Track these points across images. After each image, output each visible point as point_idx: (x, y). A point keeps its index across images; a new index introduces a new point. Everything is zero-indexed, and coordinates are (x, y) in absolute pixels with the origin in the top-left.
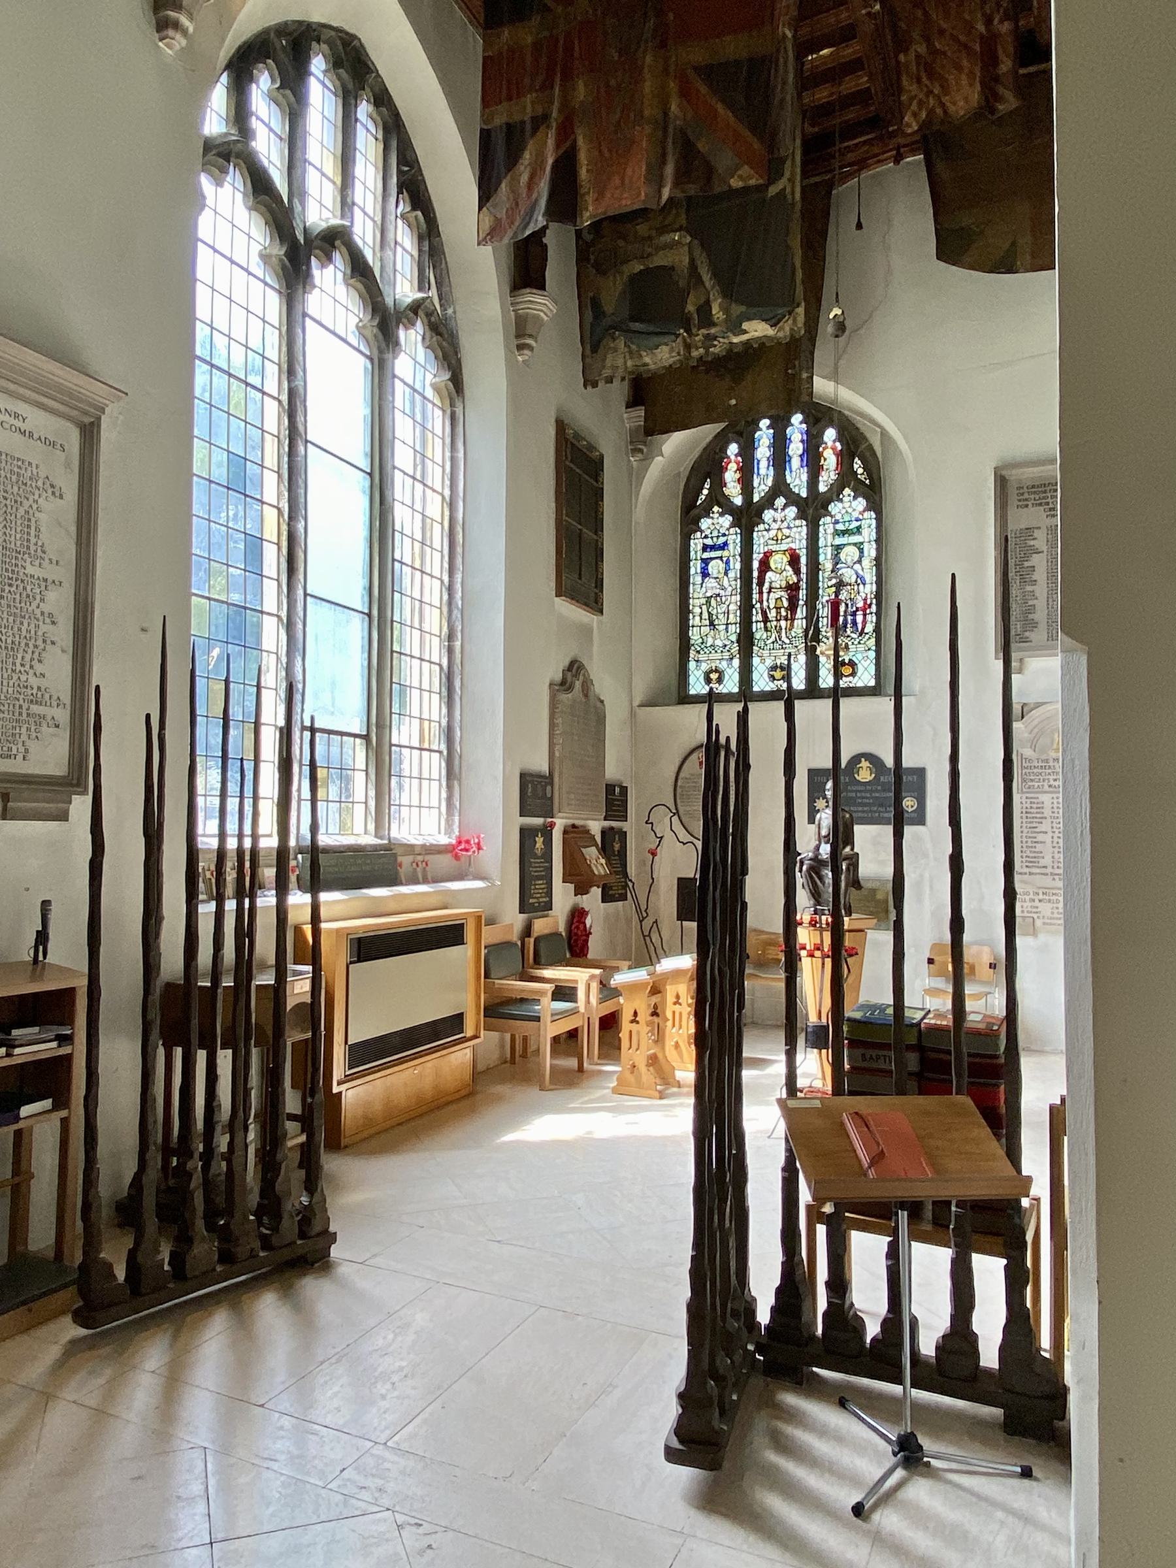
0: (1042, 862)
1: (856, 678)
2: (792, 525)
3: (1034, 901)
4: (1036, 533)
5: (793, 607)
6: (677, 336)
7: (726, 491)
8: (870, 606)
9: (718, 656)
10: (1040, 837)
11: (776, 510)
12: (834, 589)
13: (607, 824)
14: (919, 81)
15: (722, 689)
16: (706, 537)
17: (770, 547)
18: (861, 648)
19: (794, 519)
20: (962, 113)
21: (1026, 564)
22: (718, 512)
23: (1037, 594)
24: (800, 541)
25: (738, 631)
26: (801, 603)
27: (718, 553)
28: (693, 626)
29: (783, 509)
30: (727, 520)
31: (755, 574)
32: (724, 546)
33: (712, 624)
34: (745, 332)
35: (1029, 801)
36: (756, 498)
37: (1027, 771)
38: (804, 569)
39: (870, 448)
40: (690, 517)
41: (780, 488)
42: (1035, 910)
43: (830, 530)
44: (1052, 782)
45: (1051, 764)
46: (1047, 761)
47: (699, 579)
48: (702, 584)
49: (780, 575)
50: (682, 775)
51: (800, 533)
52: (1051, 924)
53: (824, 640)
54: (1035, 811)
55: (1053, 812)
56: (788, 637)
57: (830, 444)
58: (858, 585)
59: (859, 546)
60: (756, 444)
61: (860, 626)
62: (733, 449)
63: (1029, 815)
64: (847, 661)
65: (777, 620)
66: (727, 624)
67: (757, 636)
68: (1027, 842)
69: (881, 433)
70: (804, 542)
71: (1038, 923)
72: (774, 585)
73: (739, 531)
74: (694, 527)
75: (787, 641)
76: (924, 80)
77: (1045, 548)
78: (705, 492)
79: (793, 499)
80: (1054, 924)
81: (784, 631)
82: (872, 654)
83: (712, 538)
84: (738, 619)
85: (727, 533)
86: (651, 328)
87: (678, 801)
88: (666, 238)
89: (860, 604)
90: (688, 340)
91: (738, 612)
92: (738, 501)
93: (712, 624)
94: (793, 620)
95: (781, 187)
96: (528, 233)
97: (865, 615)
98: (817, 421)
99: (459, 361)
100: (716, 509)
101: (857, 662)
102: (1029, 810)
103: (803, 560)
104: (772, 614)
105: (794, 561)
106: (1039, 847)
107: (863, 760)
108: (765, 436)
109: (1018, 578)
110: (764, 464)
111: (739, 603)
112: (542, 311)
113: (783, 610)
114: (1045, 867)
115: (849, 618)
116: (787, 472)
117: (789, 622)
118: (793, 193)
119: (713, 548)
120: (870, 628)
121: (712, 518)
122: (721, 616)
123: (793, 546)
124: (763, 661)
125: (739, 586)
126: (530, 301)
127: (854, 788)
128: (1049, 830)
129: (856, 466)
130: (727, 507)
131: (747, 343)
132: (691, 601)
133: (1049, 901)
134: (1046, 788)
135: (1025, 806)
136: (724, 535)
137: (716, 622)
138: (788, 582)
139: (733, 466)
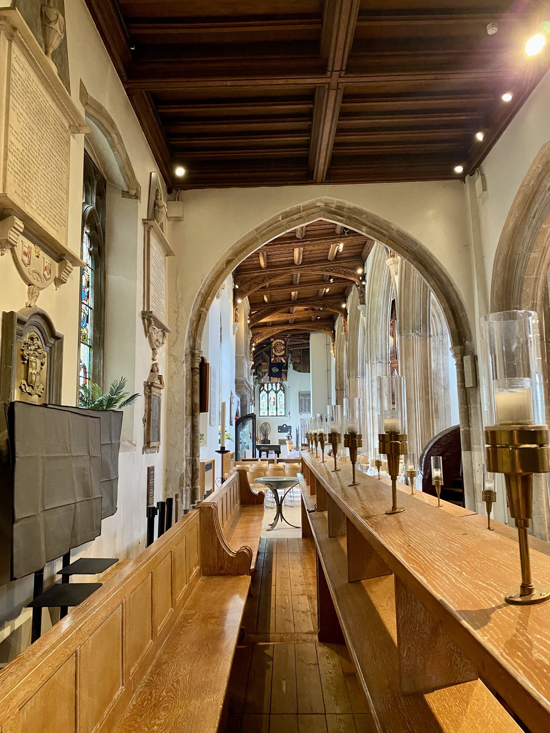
40: (260, 392)
41: (272, 389)
49: (272, 400)
79: (274, 391)
92: (267, 390)
130: (265, 391)
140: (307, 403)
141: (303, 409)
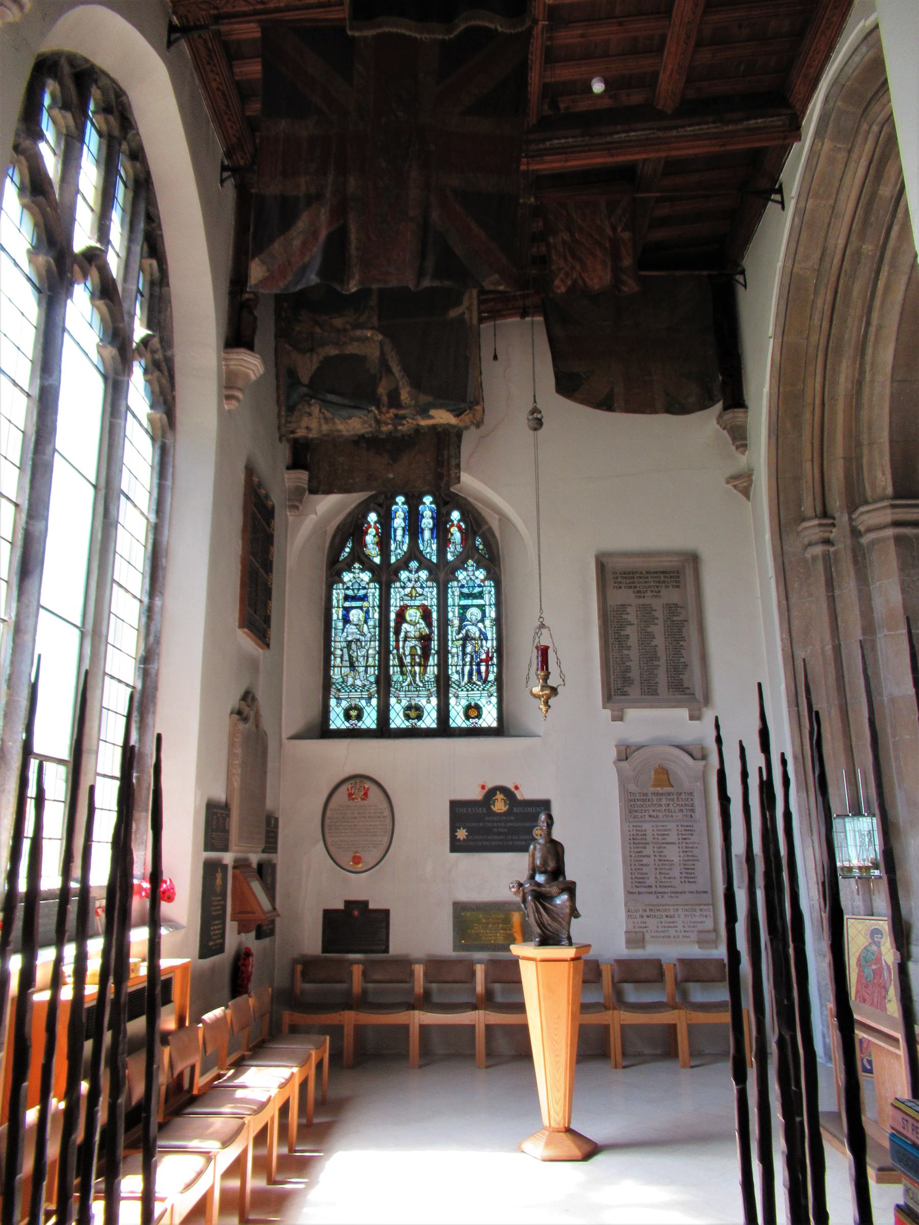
0: (648, 882)
1: (481, 720)
2: (424, 585)
3: (642, 917)
4: (629, 610)
5: (426, 654)
6: (369, 411)
7: (367, 552)
8: (491, 659)
9: (358, 694)
10: (645, 861)
11: (410, 572)
12: (461, 642)
13: (265, 856)
14: (565, 259)
15: (362, 725)
16: (348, 588)
17: (406, 602)
18: (485, 693)
19: (427, 581)
20: (597, 287)
21: (622, 633)
22: (359, 568)
23: (632, 657)
24: (432, 599)
25: (376, 672)
26: (433, 651)
27: (359, 604)
28: (334, 667)
29: (417, 572)
30: (366, 576)
31: (392, 624)
32: (364, 598)
33: (352, 666)
34: (432, 417)
35: (634, 828)
36: (393, 560)
37: (632, 803)
38: (435, 623)
39: (490, 530)
41: (414, 553)
42: (644, 925)
43: (457, 593)
44: (651, 813)
45: (650, 797)
46: (646, 794)
47: (340, 624)
48: (343, 630)
50: (331, 805)
51: (431, 592)
52: (657, 937)
53: (453, 685)
54: (640, 837)
55: (654, 839)
56: (421, 681)
57: (455, 522)
58: (482, 640)
59: (481, 607)
60: (393, 515)
61: (484, 675)
62: (373, 517)
63: (636, 841)
64: (473, 704)
65: (412, 666)
66: (366, 667)
67: (395, 679)
68: (635, 865)
69: (500, 520)
70: (435, 600)
71: (647, 937)
72: (409, 635)
73: (377, 586)
74: (337, 578)
75: (421, 685)
76: (569, 258)
77: (635, 622)
78: (347, 550)
80: (660, 937)
81: (418, 675)
82: (494, 700)
83: (353, 590)
84: (377, 662)
85: (367, 586)
86: (346, 402)
87: (327, 831)
88: (358, 333)
89: (484, 656)
90: (379, 417)
91: (377, 656)
93: (352, 666)
94: (426, 666)
95: (460, 312)
96: (299, 287)
97: (487, 666)
98: (446, 503)
99: (174, 398)
100: (357, 565)
101: (482, 706)
102: (635, 837)
103: (435, 615)
104: (408, 660)
105: (426, 615)
106: (645, 869)
107: (498, 792)
108: (400, 510)
109: (617, 643)
110: (399, 532)
111: (377, 649)
112: (251, 369)
113: (417, 657)
114: (650, 887)
115: (474, 667)
116: (420, 541)
117: (422, 668)
118: (471, 318)
119: (354, 598)
120: (491, 677)
121: (354, 573)
122: (361, 659)
123: (425, 603)
124: (399, 701)
125: (377, 633)
126: (242, 359)
127: (490, 818)
128: (652, 854)
129: (477, 543)
130: (367, 565)
131: (434, 427)
132: (333, 643)
133: (655, 916)
134: (647, 818)
135: (632, 833)
136: (364, 588)
137: (356, 664)
138: (421, 634)
139: (372, 531)
140: (658, 630)
141: (635, 674)
